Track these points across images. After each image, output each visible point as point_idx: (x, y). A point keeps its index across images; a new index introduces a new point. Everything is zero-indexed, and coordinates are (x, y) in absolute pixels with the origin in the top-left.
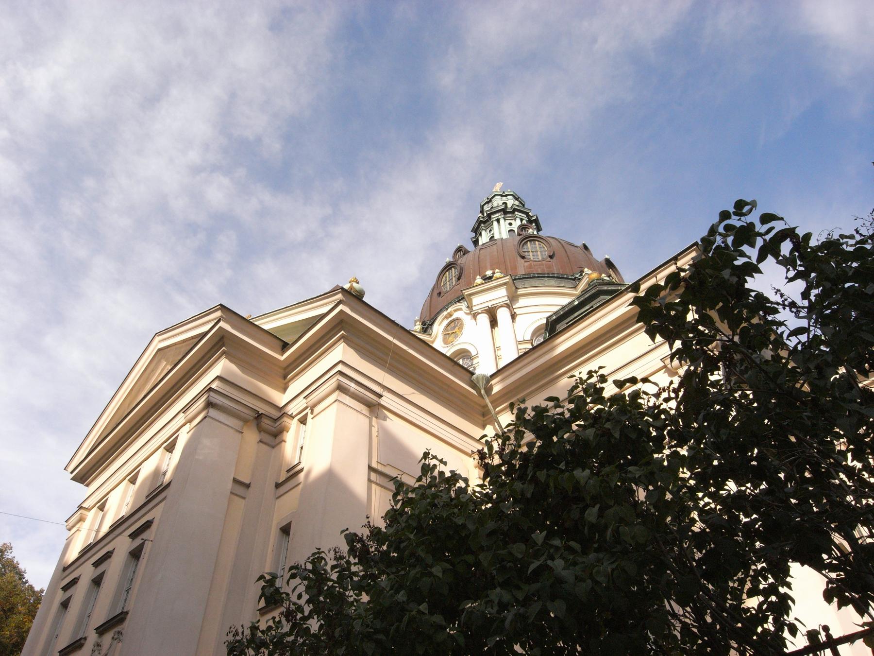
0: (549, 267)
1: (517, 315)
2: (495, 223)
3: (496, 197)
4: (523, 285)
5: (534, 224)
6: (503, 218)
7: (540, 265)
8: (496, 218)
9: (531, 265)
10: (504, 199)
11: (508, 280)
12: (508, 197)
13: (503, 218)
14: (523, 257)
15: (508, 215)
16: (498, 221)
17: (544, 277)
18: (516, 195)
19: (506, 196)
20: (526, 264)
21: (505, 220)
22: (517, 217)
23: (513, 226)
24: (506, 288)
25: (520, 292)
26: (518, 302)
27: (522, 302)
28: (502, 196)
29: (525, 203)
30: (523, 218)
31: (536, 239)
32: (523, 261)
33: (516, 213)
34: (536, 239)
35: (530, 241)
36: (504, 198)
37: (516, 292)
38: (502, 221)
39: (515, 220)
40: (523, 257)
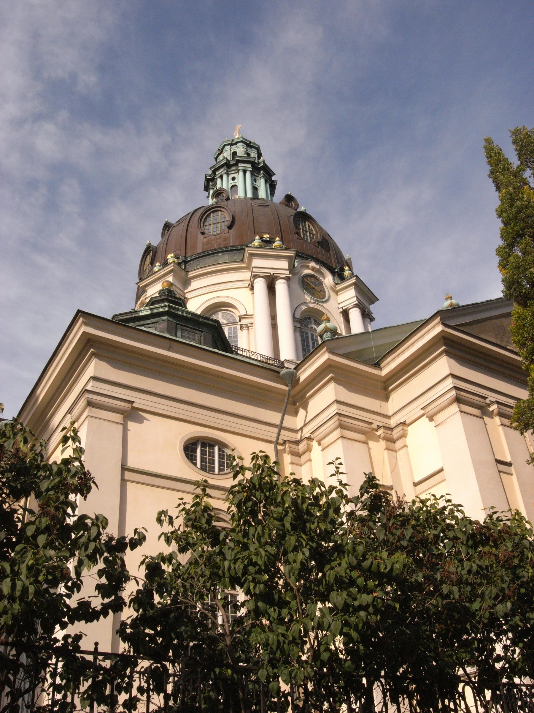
0: (225, 239)
1: (188, 299)
3: (226, 147)
4: (199, 265)
5: (262, 172)
6: (226, 173)
7: (217, 239)
8: (219, 175)
9: (209, 240)
10: (234, 149)
11: (172, 267)
12: (238, 144)
13: (226, 173)
14: (203, 233)
15: (233, 168)
16: (221, 177)
17: (219, 252)
18: (246, 140)
19: (236, 143)
20: (205, 240)
21: (228, 175)
22: (239, 170)
23: (236, 181)
24: (173, 275)
25: (191, 274)
26: (190, 285)
27: (195, 284)
28: (231, 145)
29: (259, 146)
30: (246, 169)
31: (218, 209)
32: (202, 236)
33: (240, 165)
34: (218, 209)
35: (213, 212)
36: (234, 146)
37: (187, 275)
38: (225, 177)
39: (238, 172)
40: (203, 233)
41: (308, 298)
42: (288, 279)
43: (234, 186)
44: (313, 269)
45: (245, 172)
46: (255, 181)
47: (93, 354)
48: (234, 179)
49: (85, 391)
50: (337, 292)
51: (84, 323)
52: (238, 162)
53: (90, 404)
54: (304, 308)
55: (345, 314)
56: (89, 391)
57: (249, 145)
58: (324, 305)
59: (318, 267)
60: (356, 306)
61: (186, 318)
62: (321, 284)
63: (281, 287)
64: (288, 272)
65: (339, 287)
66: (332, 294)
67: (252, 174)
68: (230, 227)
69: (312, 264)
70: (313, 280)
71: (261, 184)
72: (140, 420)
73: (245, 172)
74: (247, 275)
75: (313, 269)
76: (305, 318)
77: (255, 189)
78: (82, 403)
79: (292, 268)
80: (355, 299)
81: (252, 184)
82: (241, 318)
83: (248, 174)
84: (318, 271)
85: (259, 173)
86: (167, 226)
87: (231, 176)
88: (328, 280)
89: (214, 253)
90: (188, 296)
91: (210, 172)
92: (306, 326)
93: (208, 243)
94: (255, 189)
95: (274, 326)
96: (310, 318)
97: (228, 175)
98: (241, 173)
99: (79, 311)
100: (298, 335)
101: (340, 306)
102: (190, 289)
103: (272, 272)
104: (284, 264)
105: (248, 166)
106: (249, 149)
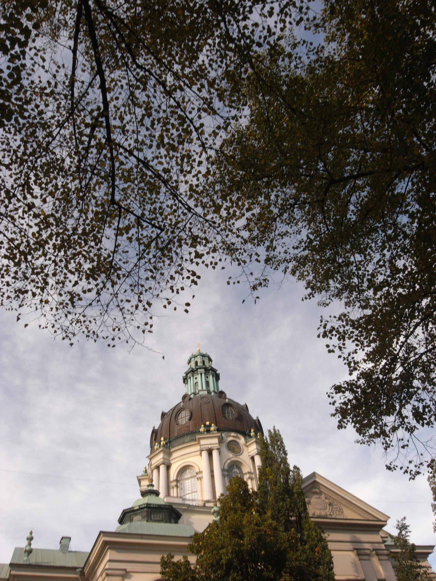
0: (188, 427)
2: (189, 380)
10: (196, 359)
16: (190, 378)
21: (193, 376)
25: (172, 450)
27: (175, 455)
28: (195, 357)
38: (192, 378)
41: (231, 455)
42: (218, 449)
43: (196, 383)
44: (233, 437)
45: (201, 374)
46: (207, 377)
47: (108, 548)
48: (196, 378)
49: (105, 570)
50: (247, 446)
51: (103, 536)
52: (197, 369)
53: (107, 575)
54: (229, 461)
55: (253, 458)
56: (107, 569)
57: (203, 356)
58: (241, 457)
59: (235, 435)
60: (257, 454)
61: (155, 508)
62: (238, 444)
63: (215, 454)
64: (218, 445)
65: (248, 444)
66: (245, 448)
67: (205, 374)
68: (190, 419)
69: (233, 434)
70: (234, 443)
71: (211, 379)
72: (130, 577)
73: (201, 374)
74: (197, 448)
75: (233, 437)
76: (231, 466)
77: (207, 383)
78: (104, 575)
79: (221, 440)
80: (256, 450)
81: (205, 380)
82: (197, 474)
83: (203, 375)
84: (236, 437)
85: (209, 373)
86: (163, 415)
87: (195, 377)
88: (242, 440)
89: (183, 436)
90: (172, 462)
91: (185, 375)
92: (232, 471)
93: (180, 429)
94: (207, 383)
95: (212, 477)
96: (233, 466)
97: (193, 376)
98: (199, 375)
99: (101, 533)
100: (227, 480)
101: (250, 454)
102: (172, 458)
103: (210, 446)
104: (216, 441)
105: (203, 371)
106: (204, 358)
